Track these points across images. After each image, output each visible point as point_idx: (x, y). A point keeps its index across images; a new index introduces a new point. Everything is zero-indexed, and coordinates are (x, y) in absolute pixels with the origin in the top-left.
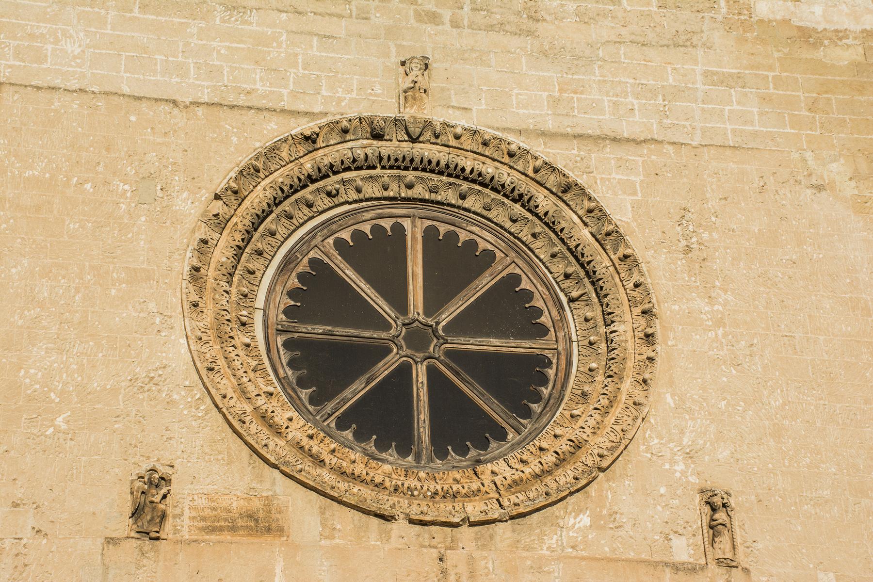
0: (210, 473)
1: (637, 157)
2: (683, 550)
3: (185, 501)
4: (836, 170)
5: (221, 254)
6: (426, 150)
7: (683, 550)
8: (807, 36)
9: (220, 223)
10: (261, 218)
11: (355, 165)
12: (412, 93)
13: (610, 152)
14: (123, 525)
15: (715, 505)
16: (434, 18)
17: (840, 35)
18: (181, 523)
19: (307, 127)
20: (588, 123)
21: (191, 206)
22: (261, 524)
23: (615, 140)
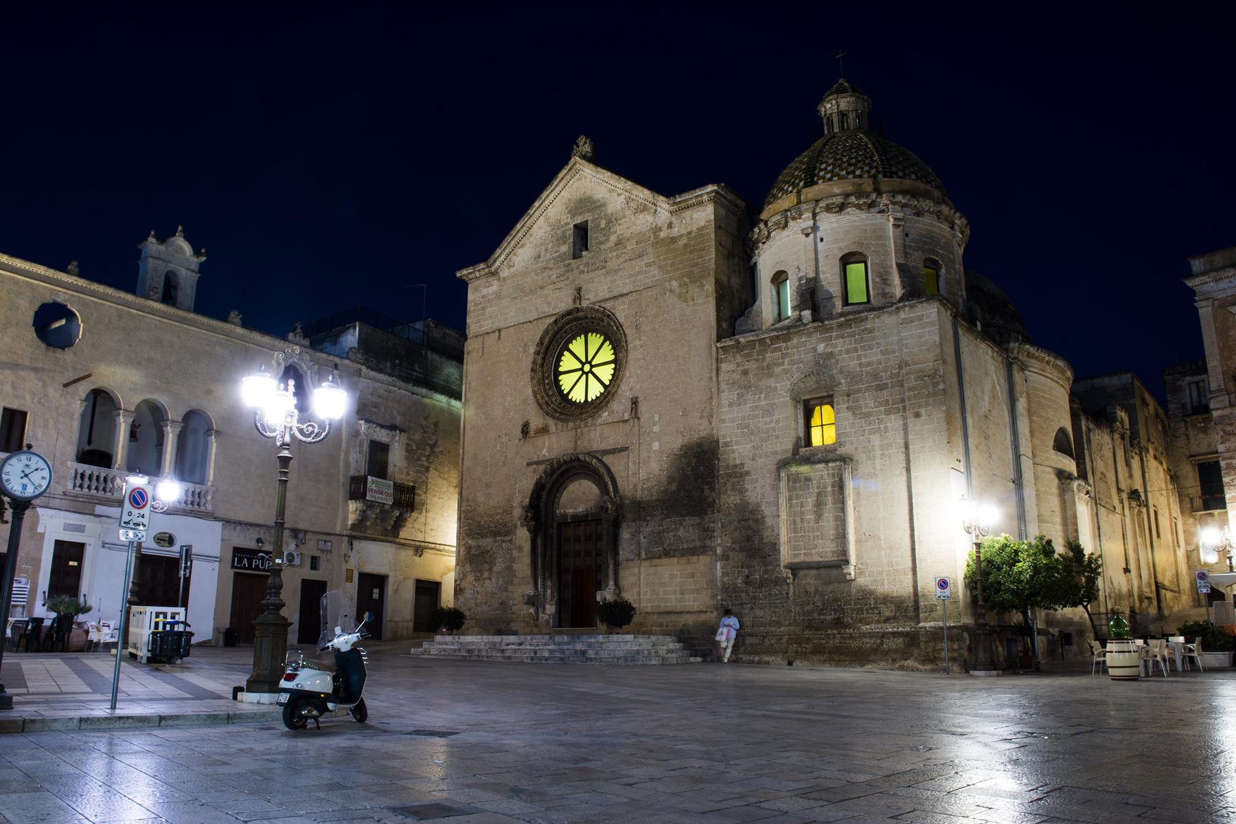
0: (536, 421)
1: (626, 299)
2: (626, 416)
3: (533, 427)
4: (675, 284)
5: (539, 361)
6: (580, 314)
7: (626, 416)
8: (673, 240)
9: (537, 353)
10: (547, 348)
11: (567, 323)
12: (575, 302)
13: (620, 300)
14: (521, 436)
15: (635, 402)
16: (583, 272)
17: (681, 236)
18: (532, 433)
19: (554, 318)
20: (616, 292)
21: (532, 350)
22: (544, 430)
23: (622, 295)
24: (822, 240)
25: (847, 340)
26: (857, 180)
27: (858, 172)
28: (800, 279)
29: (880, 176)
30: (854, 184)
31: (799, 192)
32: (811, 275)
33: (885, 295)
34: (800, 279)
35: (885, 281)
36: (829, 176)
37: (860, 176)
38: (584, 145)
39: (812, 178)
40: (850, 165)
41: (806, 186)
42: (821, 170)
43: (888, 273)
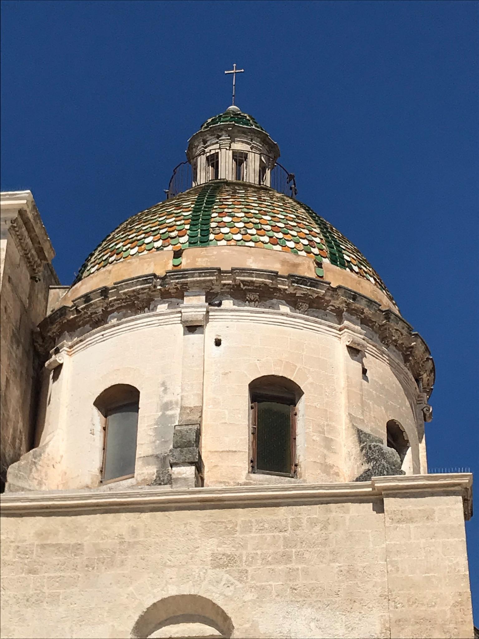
24: (218, 343)
25: (268, 535)
26: (289, 256)
27: (291, 244)
29: (326, 261)
30: (284, 262)
31: (178, 254)
32: (192, 402)
33: (327, 468)
34: (166, 406)
35: (328, 443)
36: (239, 237)
37: (295, 251)
39: (206, 233)
40: (276, 229)
41: (192, 244)
42: (222, 224)
43: (332, 429)
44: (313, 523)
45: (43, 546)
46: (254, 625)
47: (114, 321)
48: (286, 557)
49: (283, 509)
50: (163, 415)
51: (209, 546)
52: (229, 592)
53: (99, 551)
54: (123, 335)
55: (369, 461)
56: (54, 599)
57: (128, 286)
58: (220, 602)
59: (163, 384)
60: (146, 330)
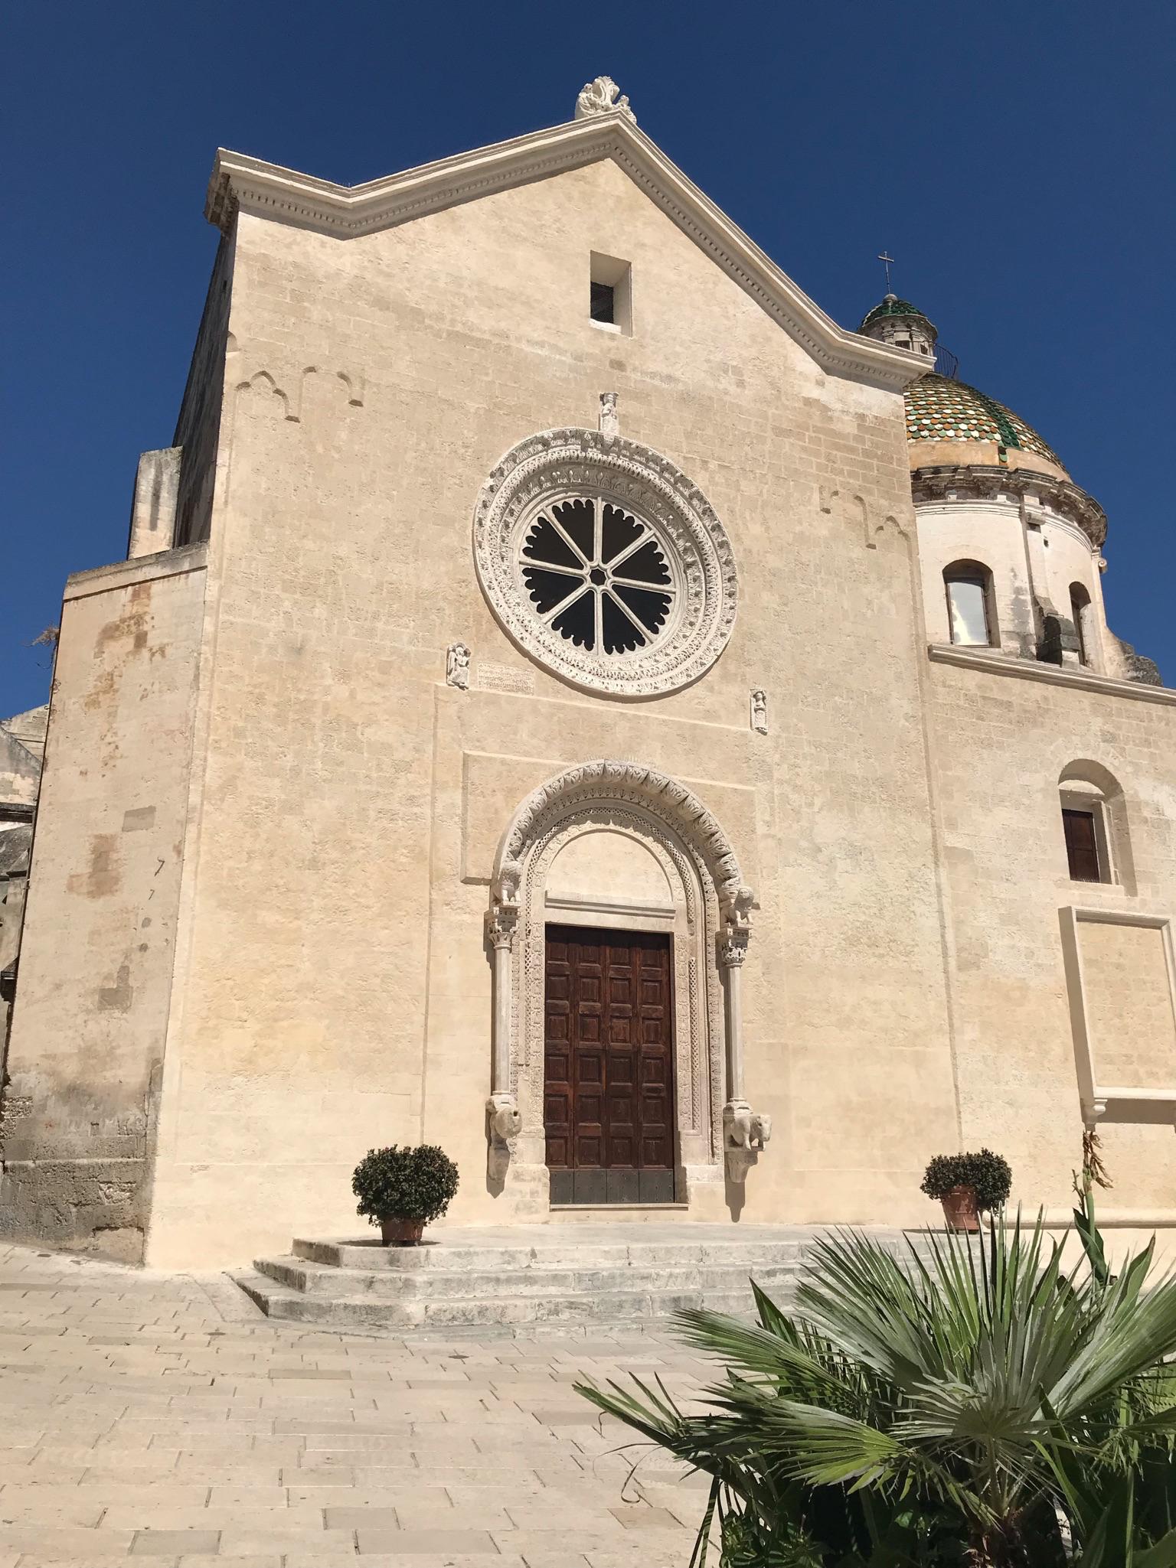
28: (1018, 591)
38: (602, 100)
44: (1160, 719)
45: (984, 698)
46: (1136, 793)
47: (953, 497)
48: (1147, 743)
49: (1139, 703)
50: (1016, 599)
51: (1097, 723)
52: (1116, 763)
53: (1026, 711)
54: (967, 514)
55: (1137, 670)
56: (1001, 746)
57: (982, 471)
58: (1111, 769)
59: (1013, 570)
60: (990, 515)
